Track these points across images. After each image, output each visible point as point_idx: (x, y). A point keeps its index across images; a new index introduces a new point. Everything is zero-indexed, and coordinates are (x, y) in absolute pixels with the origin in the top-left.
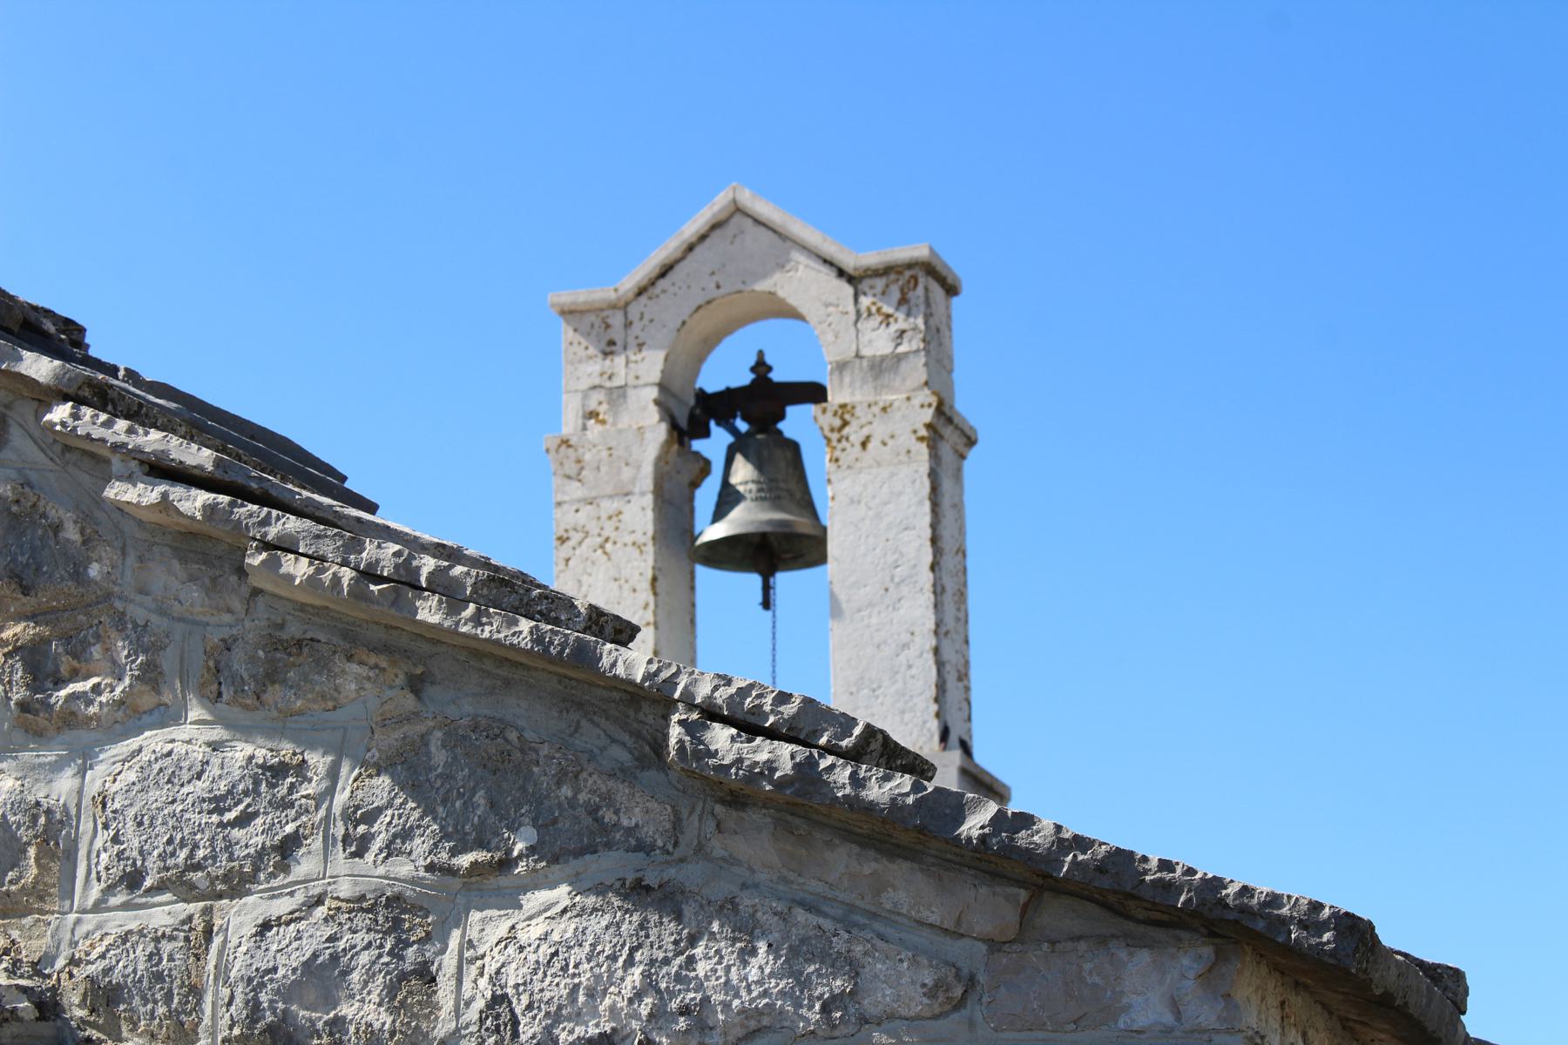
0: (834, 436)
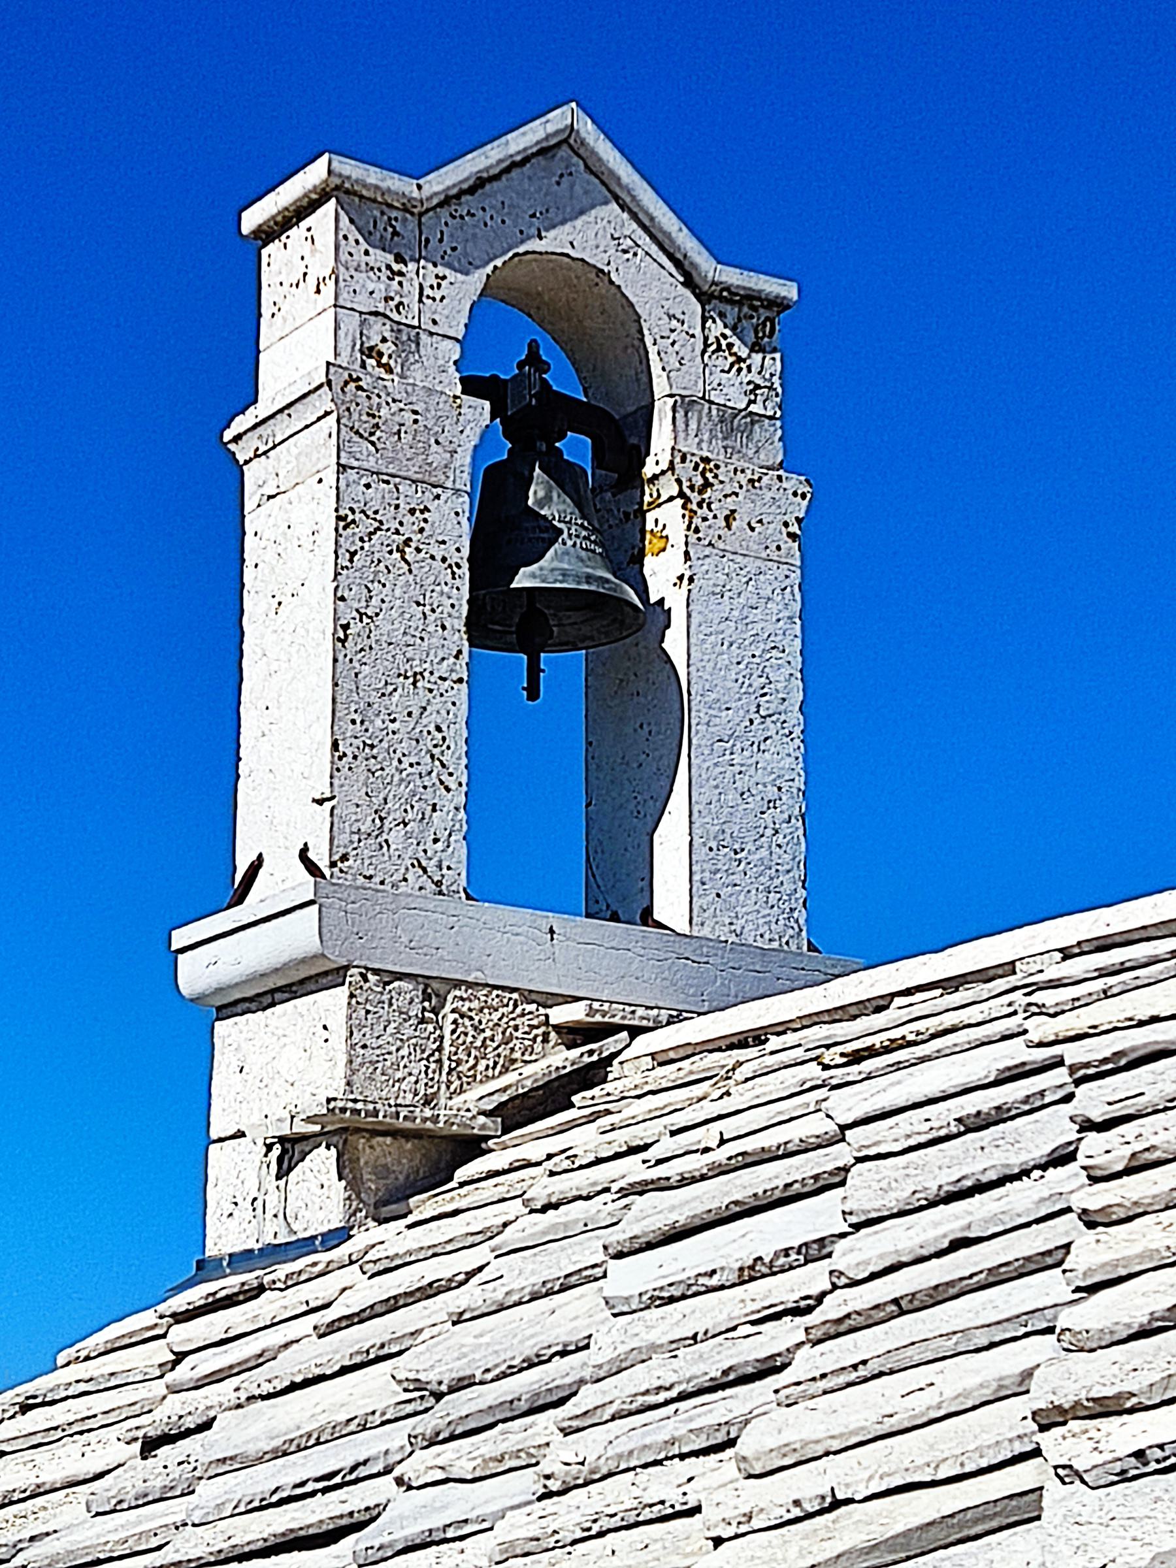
0: (695, 497)
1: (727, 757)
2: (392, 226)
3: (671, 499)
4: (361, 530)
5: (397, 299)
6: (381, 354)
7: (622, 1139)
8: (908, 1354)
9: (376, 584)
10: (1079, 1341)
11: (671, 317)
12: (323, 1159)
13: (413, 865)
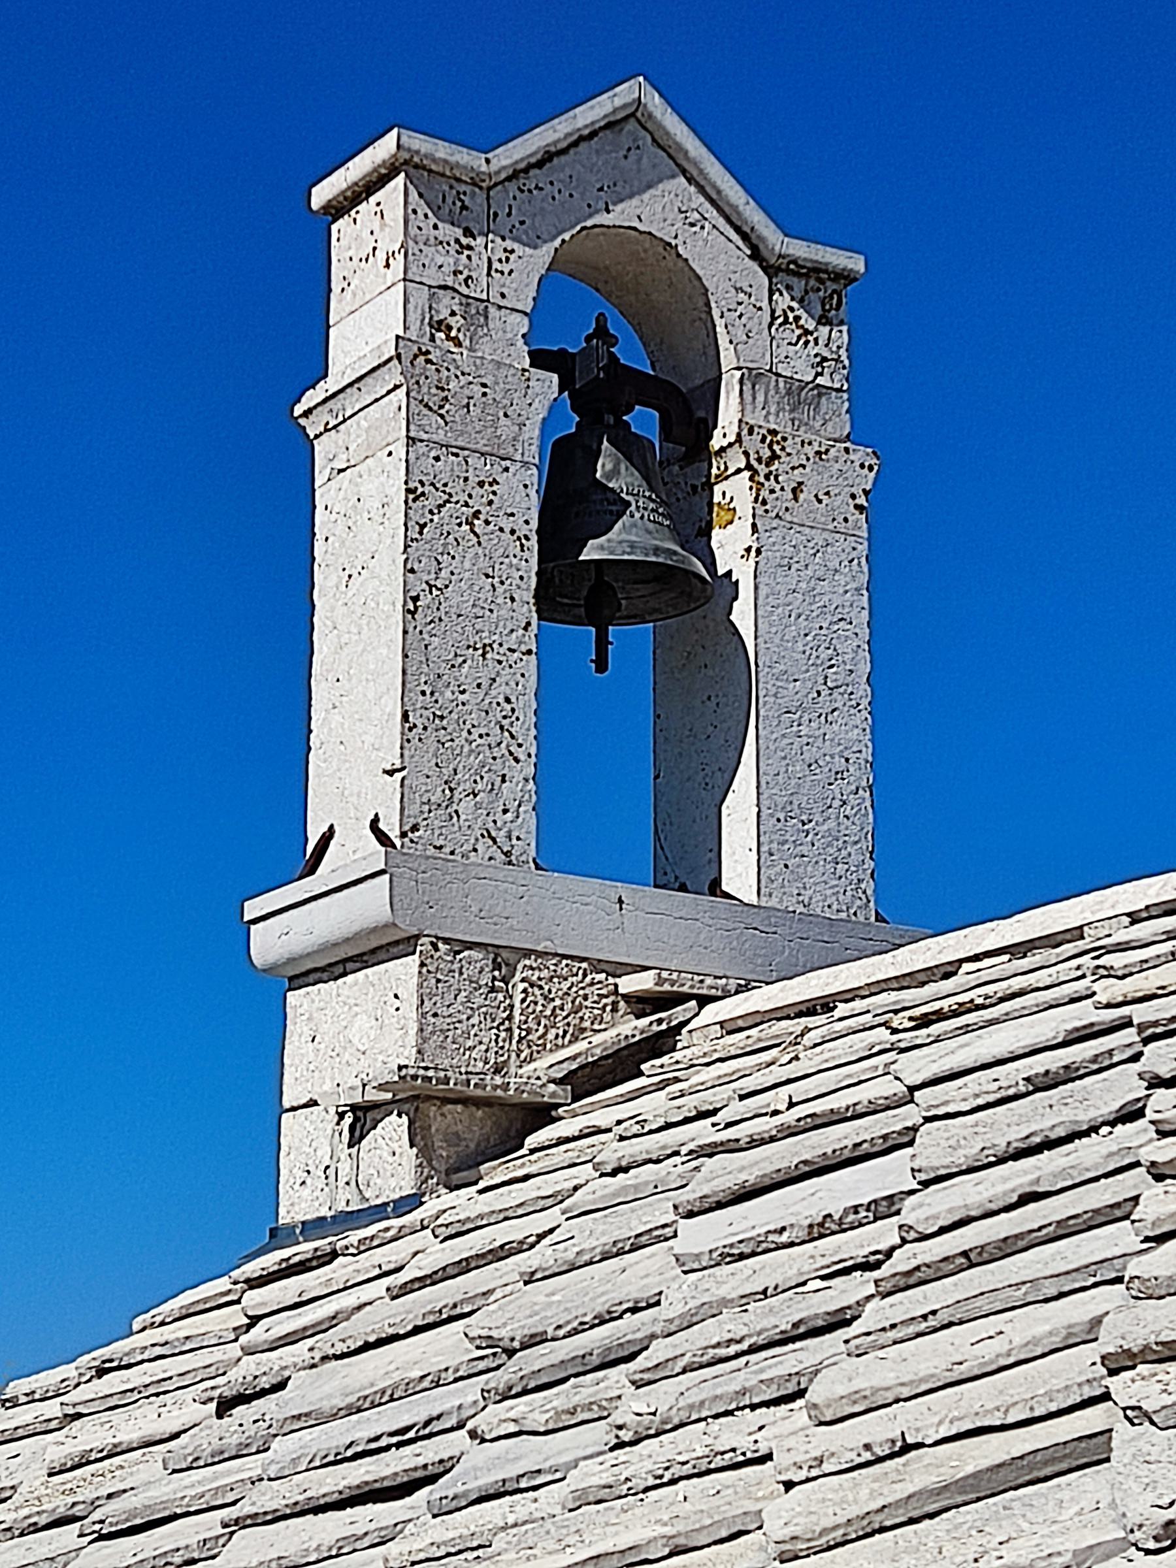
0: (762, 469)
1: (795, 729)
2: (460, 200)
3: (739, 471)
4: (430, 503)
5: (466, 273)
6: (450, 328)
7: (690, 1104)
8: (977, 1305)
9: (445, 556)
10: (1148, 1288)
11: (739, 290)
12: (394, 1127)
13: (483, 836)
